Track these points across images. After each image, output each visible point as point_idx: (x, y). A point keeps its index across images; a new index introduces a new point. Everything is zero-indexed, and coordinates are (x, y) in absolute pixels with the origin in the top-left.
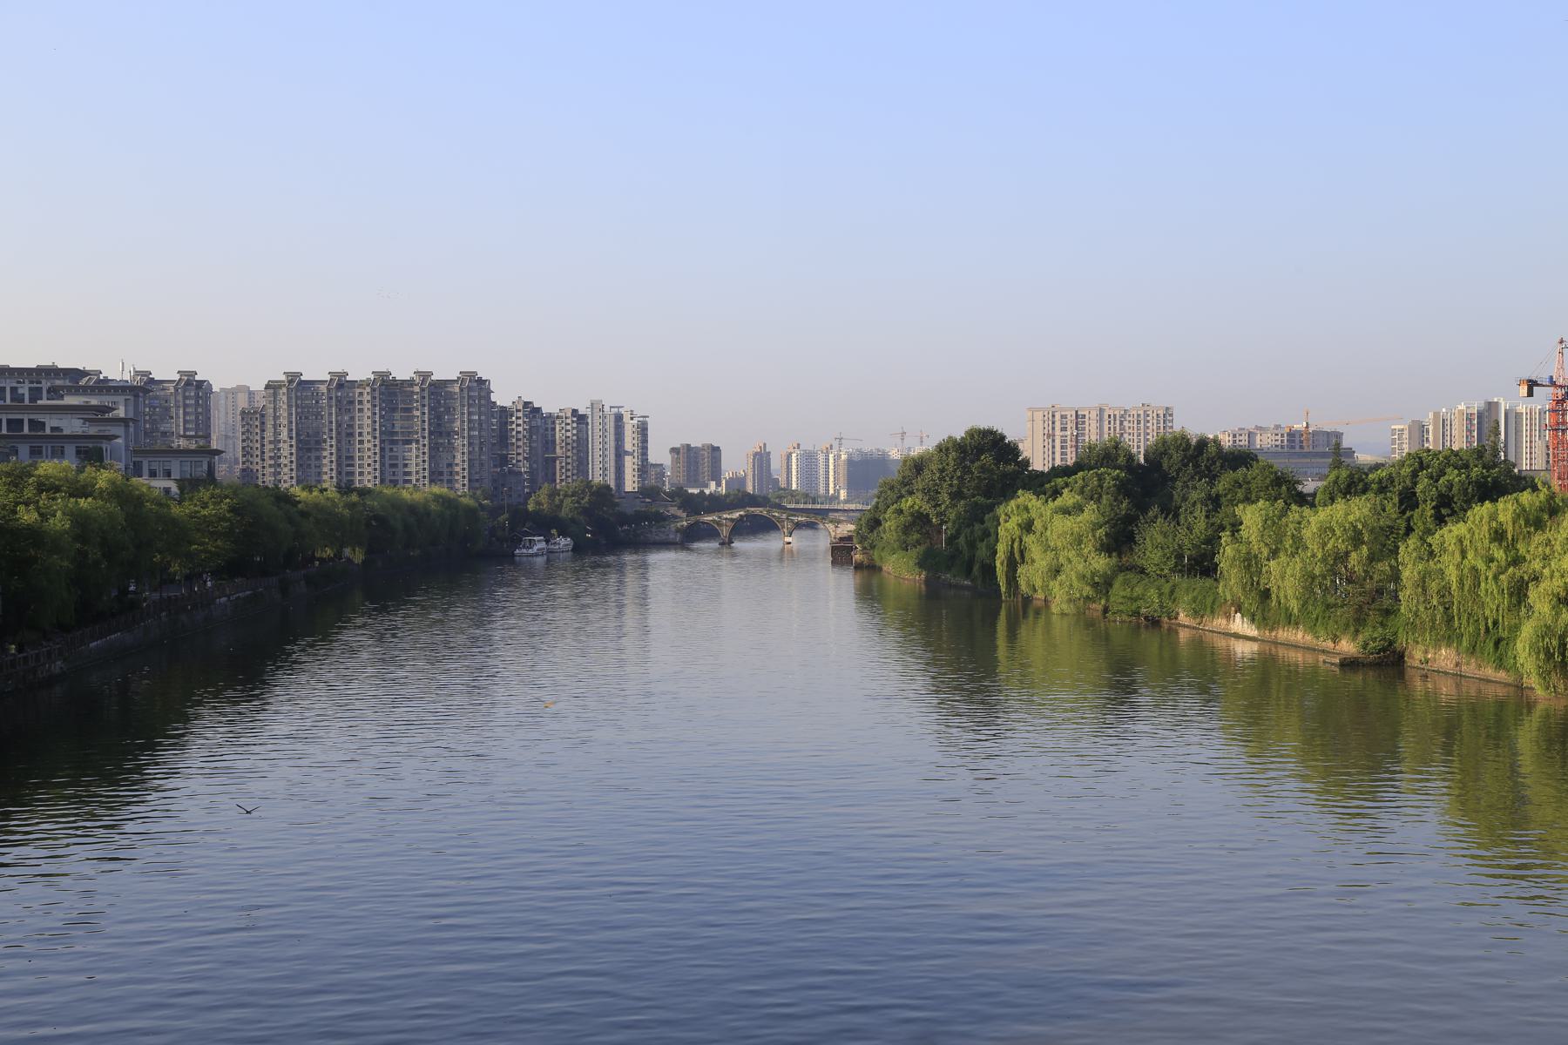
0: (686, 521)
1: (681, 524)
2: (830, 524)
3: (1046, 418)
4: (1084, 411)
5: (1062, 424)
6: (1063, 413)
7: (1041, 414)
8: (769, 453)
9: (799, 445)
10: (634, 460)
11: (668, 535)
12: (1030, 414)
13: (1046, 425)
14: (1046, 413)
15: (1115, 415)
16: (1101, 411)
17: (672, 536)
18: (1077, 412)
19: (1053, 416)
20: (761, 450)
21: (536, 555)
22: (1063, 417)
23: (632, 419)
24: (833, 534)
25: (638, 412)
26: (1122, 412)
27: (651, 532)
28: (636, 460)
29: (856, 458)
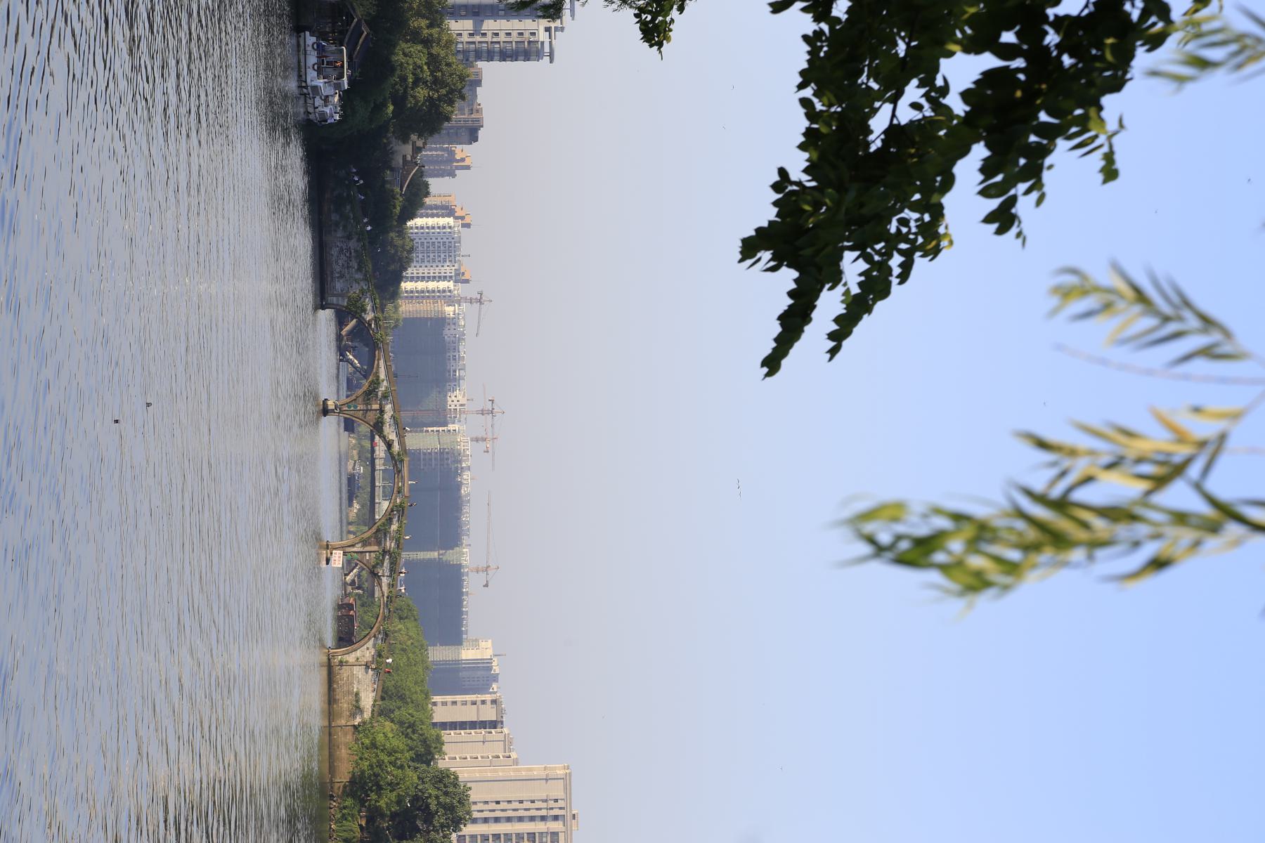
0: (376, 319)
1: (369, 308)
2: (373, 651)
3: (552, 804)
5: (541, 834)
7: (559, 794)
8: (454, 175)
9: (467, 226)
10: (465, 34)
11: (342, 276)
12: (561, 772)
13: (538, 804)
14: (561, 803)
17: (339, 285)
19: (556, 818)
20: (458, 161)
21: (301, 78)
23: (548, 29)
24: (351, 658)
25: (560, 40)
27: (349, 238)
28: (465, 38)
29: (448, 332)
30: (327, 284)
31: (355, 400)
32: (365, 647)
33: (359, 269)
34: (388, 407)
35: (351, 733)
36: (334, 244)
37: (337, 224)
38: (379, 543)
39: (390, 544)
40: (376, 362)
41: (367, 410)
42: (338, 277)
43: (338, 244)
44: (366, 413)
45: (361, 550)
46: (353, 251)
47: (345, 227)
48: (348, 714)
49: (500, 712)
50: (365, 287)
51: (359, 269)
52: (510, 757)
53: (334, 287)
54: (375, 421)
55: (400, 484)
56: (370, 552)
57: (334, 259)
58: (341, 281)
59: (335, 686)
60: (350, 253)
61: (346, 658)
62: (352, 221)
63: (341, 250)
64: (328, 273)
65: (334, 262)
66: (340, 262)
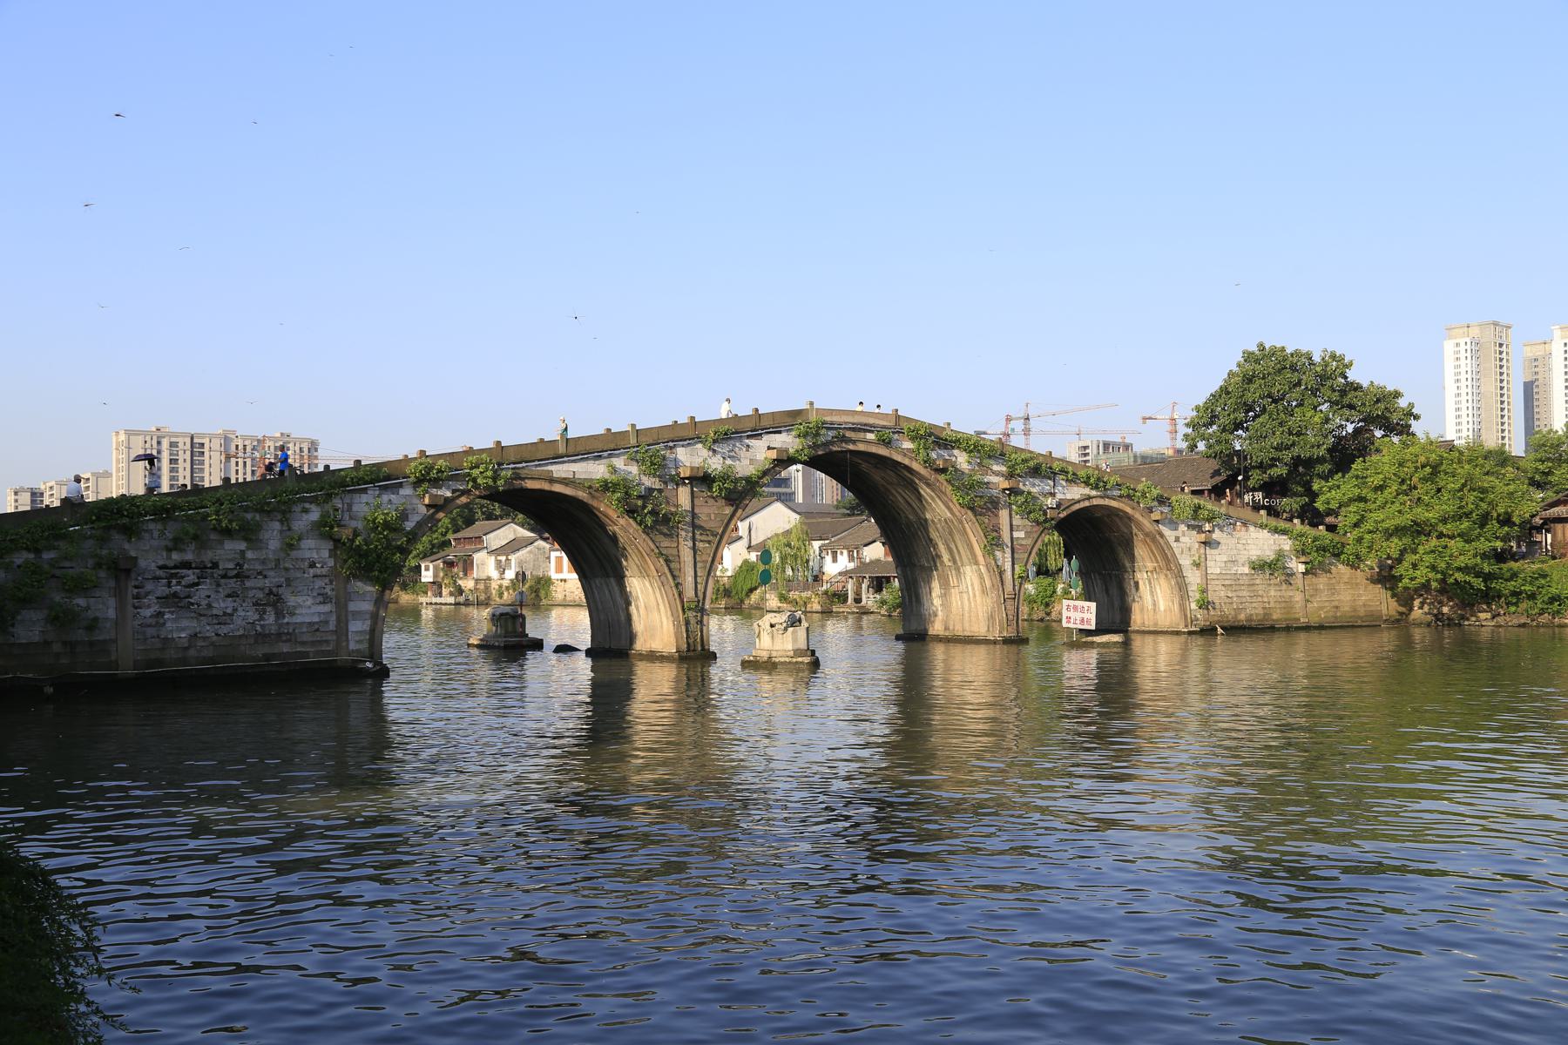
4: (203, 438)
5: (171, 454)
6: (173, 440)
7: (141, 439)
11: (274, 600)
12: (122, 437)
14: (148, 439)
15: (245, 446)
16: (227, 440)
17: (306, 609)
18: (192, 438)
19: (159, 443)
22: (173, 445)
24: (1193, 578)
26: (255, 443)
27: (122, 569)
30: (306, 654)
31: (667, 561)
32: (1174, 545)
33: (249, 533)
34: (689, 458)
35: (1315, 580)
36: (150, 631)
37: (61, 619)
38: (994, 504)
39: (996, 478)
40: (558, 488)
41: (694, 526)
42: (279, 614)
43: (147, 613)
44: (701, 527)
45: (1008, 551)
46: (176, 556)
47: (80, 586)
48: (1284, 586)
49: (23, 490)
50: (315, 515)
51: (249, 533)
52: (88, 479)
53: (315, 628)
54: (722, 502)
55: (871, 436)
56: (1012, 530)
57: (209, 631)
58: (292, 600)
59: (1242, 617)
60: (186, 565)
61: (1195, 595)
62: (47, 555)
63: (172, 600)
64: (261, 650)
65: (224, 630)
66: (222, 605)
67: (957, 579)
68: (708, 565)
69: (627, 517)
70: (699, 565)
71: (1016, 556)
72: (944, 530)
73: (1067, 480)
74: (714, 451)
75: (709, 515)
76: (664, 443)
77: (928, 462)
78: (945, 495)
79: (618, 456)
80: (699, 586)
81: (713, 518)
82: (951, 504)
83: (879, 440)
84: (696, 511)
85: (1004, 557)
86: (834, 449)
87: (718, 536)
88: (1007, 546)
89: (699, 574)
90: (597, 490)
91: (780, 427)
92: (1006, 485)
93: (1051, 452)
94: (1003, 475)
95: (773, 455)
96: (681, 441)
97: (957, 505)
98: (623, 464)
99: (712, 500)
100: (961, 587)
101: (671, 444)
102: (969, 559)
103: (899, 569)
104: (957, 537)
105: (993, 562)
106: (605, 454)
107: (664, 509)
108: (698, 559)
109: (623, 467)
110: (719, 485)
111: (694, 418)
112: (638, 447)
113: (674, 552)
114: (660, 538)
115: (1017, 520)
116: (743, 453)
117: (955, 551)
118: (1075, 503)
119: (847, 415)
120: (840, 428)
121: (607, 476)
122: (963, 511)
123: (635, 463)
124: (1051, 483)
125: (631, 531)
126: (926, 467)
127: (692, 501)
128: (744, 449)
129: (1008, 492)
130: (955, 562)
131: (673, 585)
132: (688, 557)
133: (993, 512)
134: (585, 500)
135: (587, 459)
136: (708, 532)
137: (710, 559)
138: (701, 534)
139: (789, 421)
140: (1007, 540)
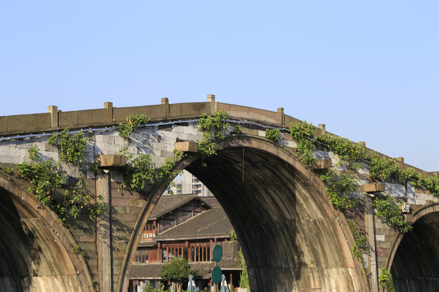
31: (86, 258)
44: (117, 222)
45: (373, 254)
54: (136, 195)
55: (262, 134)
56: (375, 234)
67: (320, 281)
68: (124, 263)
69: (48, 208)
70: (115, 262)
71: (379, 260)
72: (311, 232)
73: (417, 187)
74: (130, 141)
75: (124, 208)
76: (84, 128)
77: (309, 162)
78: (321, 194)
79: (40, 140)
80: (115, 286)
81: (128, 211)
82: (325, 205)
83: (270, 138)
84: (114, 203)
85: (370, 261)
86: (232, 145)
87: (133, 232)
88: (372, 249)
89: (115, 272)
90: (20, 177)
91: (188, 119)
92: (372, 188)
93: (403, 159)
94: (367, 180)
95: (185, 147)
96: (100, 127)
97: (332, 207)
98: (44, 149)
99: (127, 192)
100: (324, 289)
101: (90, 131)
102: (336, 262)
103: (252, 270)
104: (325, 239)
105: (361, 265)
106: (27, 137)
107: (88, 201)
108: (114, 256)
109: (45, 153)
110: (140, 176)
111: (112, 103)
112: (60, 131)
113: (92, 248)
114: (79, 232)
115: (379, 225)
116: (155, 145)
117: (320, 251)
118: (423, 209)
119: (244, 111)
120: (237, 124)
121: (29, 162)
122: (337, 212)
123: (56, 149)
124: (404, 188)
125: (51, 224)
126: (307, 168)
127: (110, 193)
128: (156, 140)
129: (372, 196)
130: (318, 263)
131: (91, 284)
132: (105, 253)
133: (361, 216)
134: (6, 188)
135: (8, 142)
136: (124, 228)
137: (125, 256)
138: (118, 230)
139: (194, 113)
140: (372, 244)
